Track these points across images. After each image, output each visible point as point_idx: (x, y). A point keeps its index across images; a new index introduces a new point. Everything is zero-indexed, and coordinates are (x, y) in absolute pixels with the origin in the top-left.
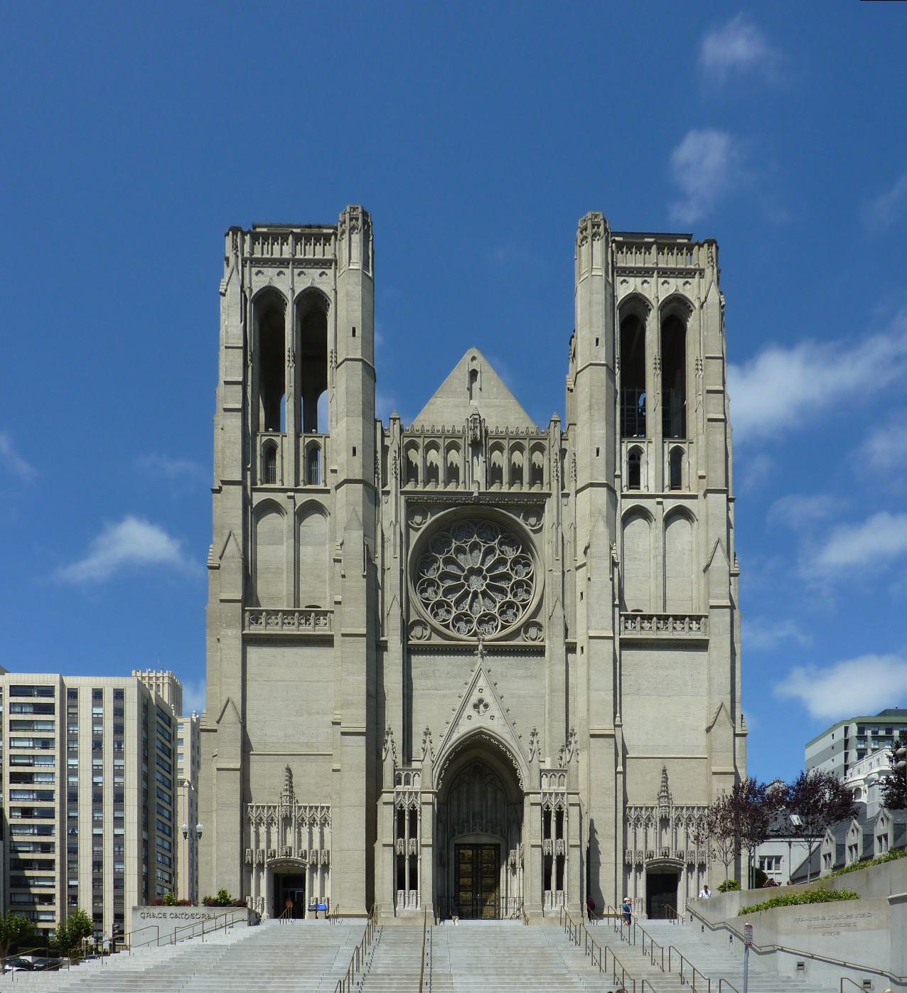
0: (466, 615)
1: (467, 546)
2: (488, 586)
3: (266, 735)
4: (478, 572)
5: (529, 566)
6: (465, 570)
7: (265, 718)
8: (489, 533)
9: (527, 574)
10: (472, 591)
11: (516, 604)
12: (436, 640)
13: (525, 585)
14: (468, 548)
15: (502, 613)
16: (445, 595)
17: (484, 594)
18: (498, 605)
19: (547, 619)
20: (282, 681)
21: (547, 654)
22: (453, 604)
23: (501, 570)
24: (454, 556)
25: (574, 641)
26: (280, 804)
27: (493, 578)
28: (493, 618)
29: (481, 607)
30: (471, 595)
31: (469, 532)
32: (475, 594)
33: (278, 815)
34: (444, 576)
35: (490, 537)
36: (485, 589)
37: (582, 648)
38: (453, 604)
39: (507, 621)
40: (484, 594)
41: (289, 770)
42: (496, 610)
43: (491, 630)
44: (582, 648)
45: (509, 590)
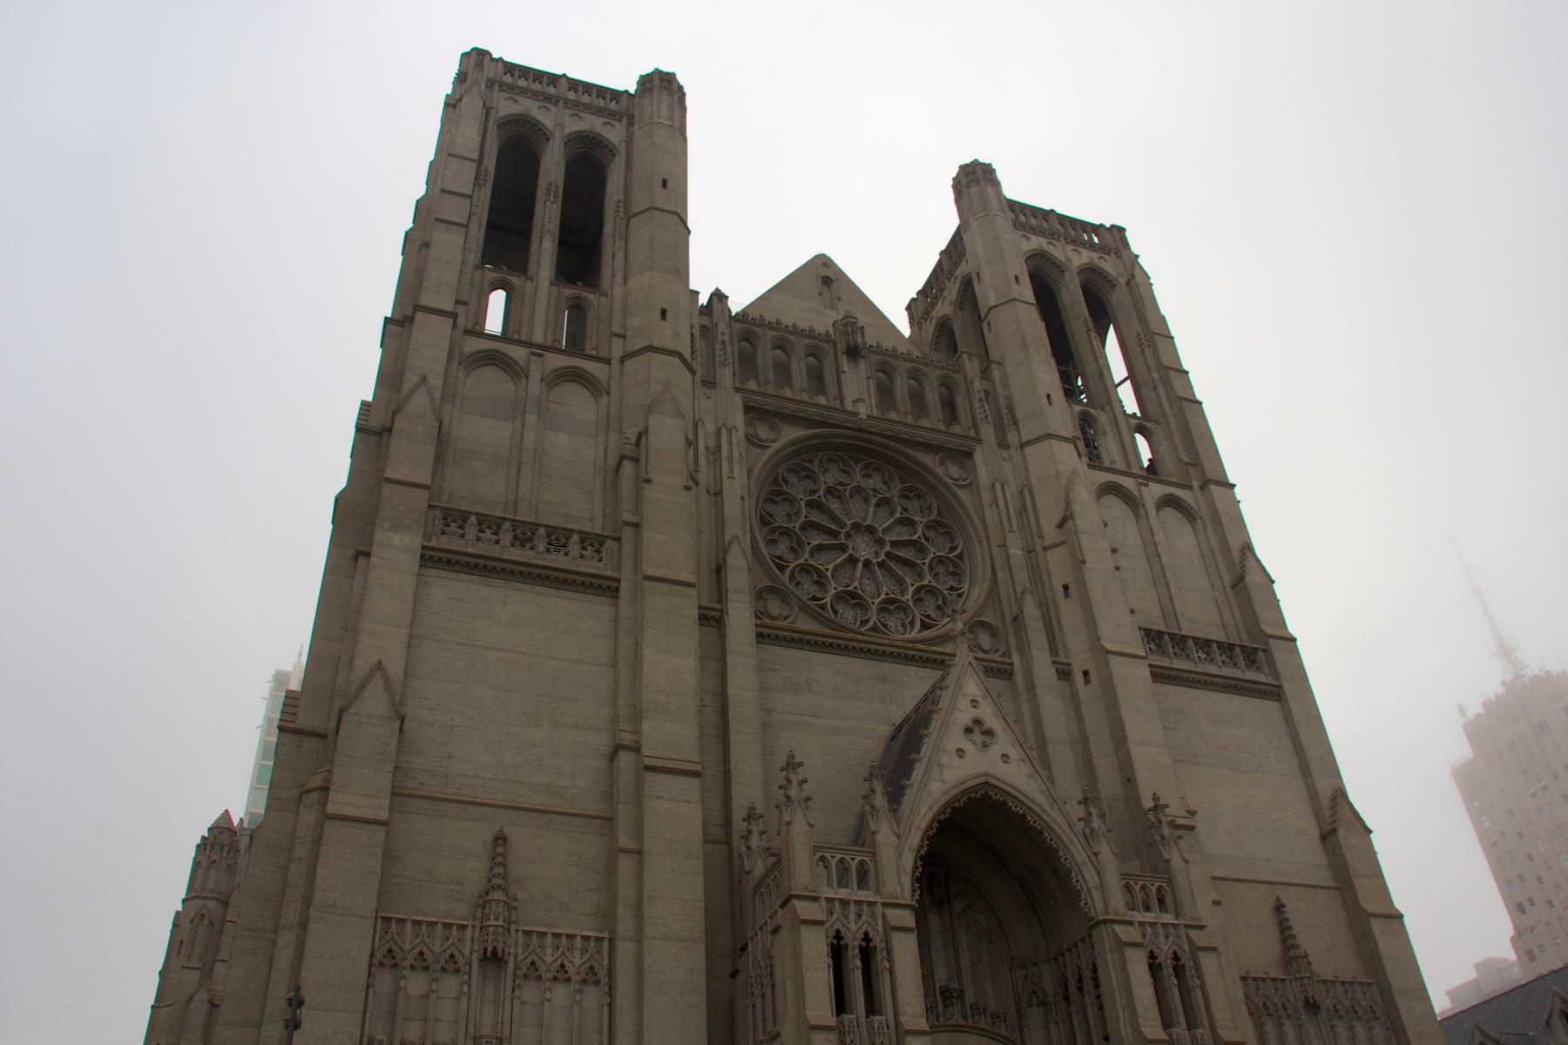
0: (853, 595)
1: (845, 490)
2: (888, 555)
3: (450, 757)
4: (871, 530)
5: (952, 539)
6: (846, 525)
7: (453, 719)
8: (878, 479)
9: (953, 549)
10: (862, 559)
11: (942, 593)
12: (806, 624)
13: (954, 566)
14: (847, 494)
15: (918, 601)
16: (812, 555)
17: (881, 565)
18: (911, 589)
19: (1008, 620)
20: (498, 650)
21: (1019, 677)
22: (829, 574)
23: (903, 534)
24: (824, 500)
25: (1066, 661)
26: (478, 923)
27: (894, 544)
28: (903, 608)
29: (877, 590)
30: (860, 565)
31: (844, 471)
32: (867, 564)
33: (470, 948)
34: (809, 526)
35: (881, 485)
36: (883, 561)
37: (1086, 673)
38: (829, 574)
39: (928, 616)
40: (881, 565)
41: (500, 839)
42: (909, 596)
43: (900, 629)
44: (1086, 673)
45: (926, 568)
